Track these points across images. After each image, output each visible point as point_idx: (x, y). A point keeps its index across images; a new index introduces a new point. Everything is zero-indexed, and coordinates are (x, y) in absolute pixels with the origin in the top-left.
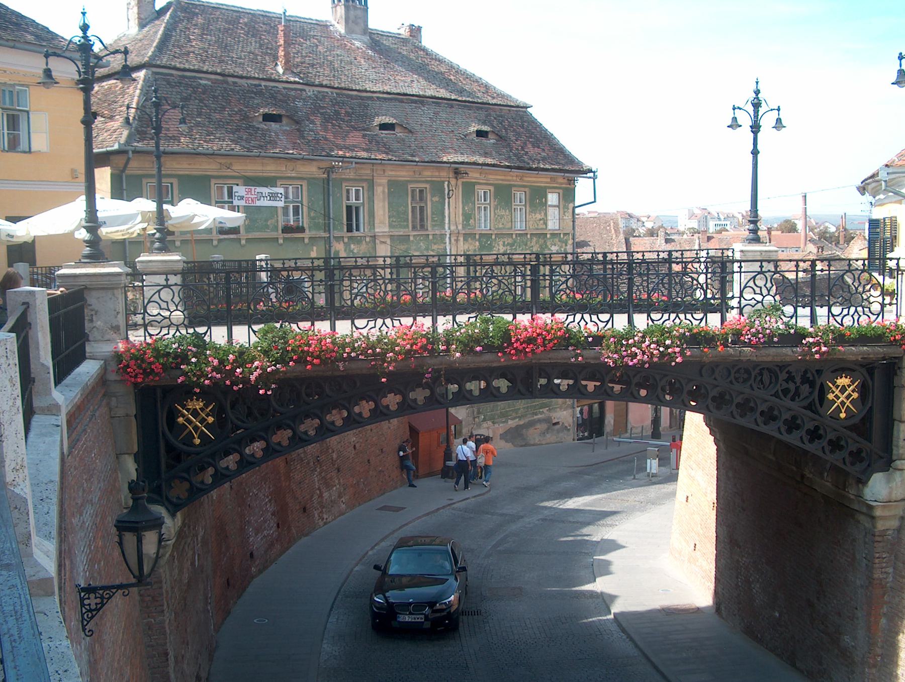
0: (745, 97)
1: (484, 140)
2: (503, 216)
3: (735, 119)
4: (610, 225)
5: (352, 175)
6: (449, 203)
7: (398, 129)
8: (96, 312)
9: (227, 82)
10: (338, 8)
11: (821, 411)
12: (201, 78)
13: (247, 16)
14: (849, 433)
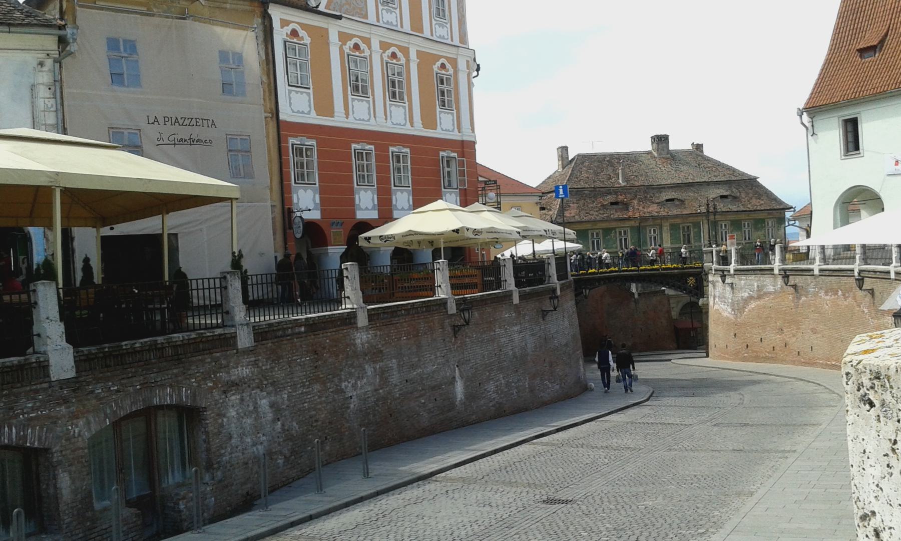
5: (651, 223)
7: (675, 200)
9: (596, 191)
10: (654, 145)
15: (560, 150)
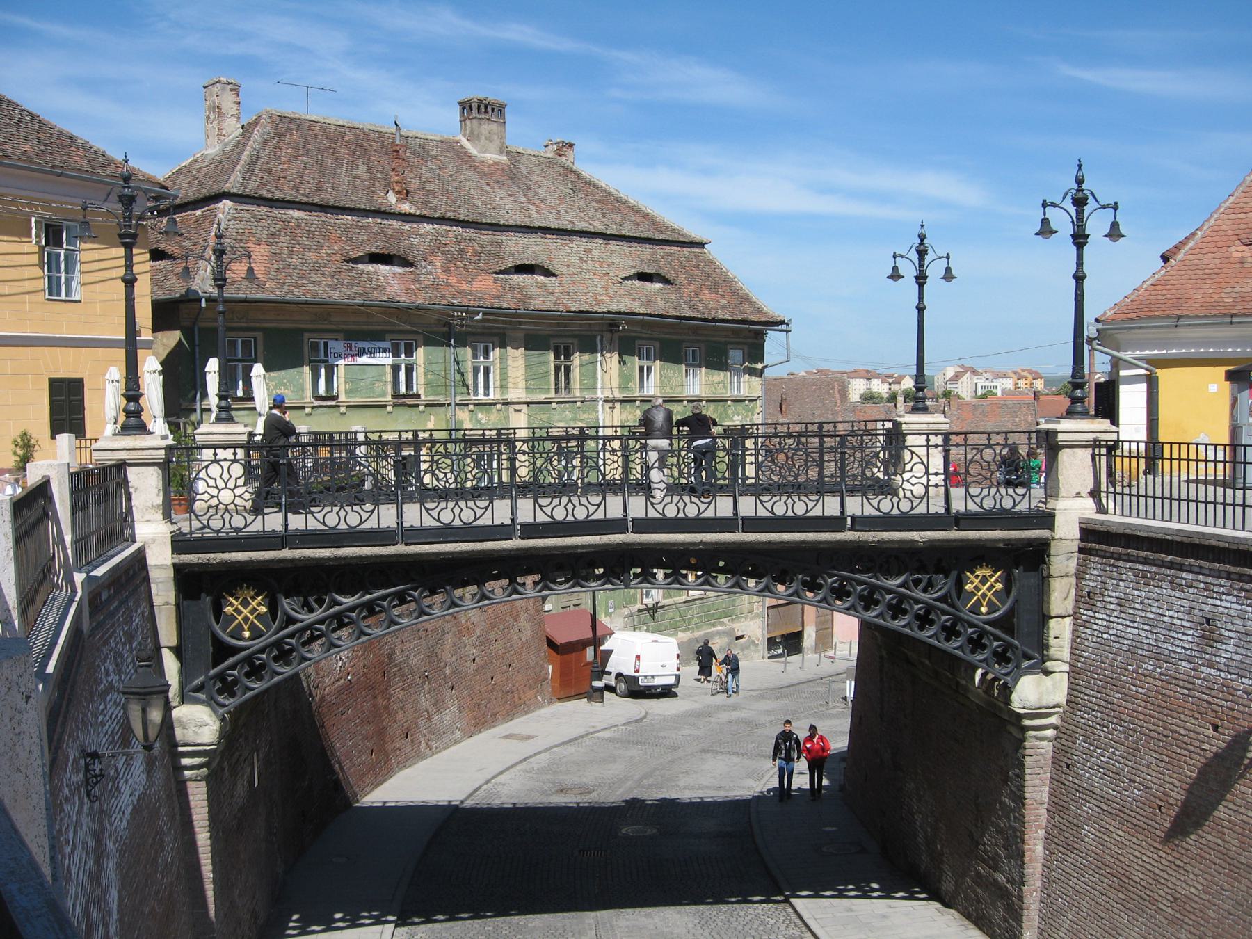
0: (907, 246)
2: (671, 377)
3: (895, 268)
4: (833, 388)
8: (136, 489)
10: (468, 122)
11: (958, 603)
13: (353, 130)
14: (988, 628)
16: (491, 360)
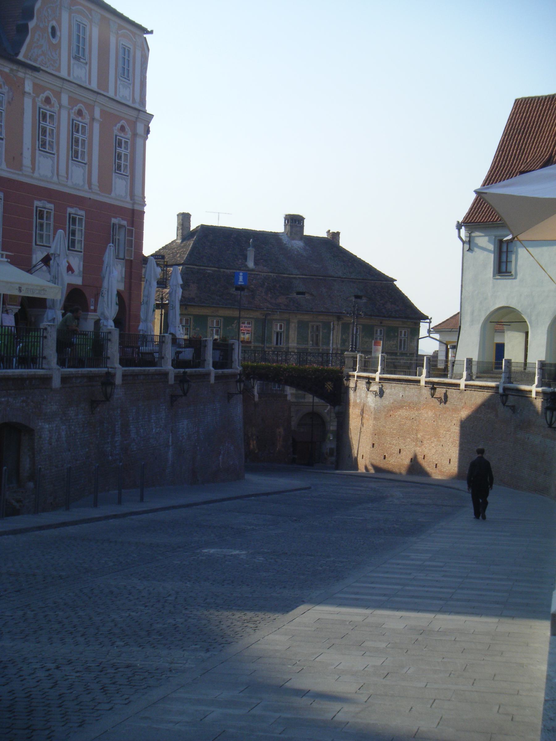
1: (359, 300)
6: (333, 333)
7: (307, 295)
10: (287, 226)
12: (207, 270)
15: (181, 217)
16: (283, 330)
